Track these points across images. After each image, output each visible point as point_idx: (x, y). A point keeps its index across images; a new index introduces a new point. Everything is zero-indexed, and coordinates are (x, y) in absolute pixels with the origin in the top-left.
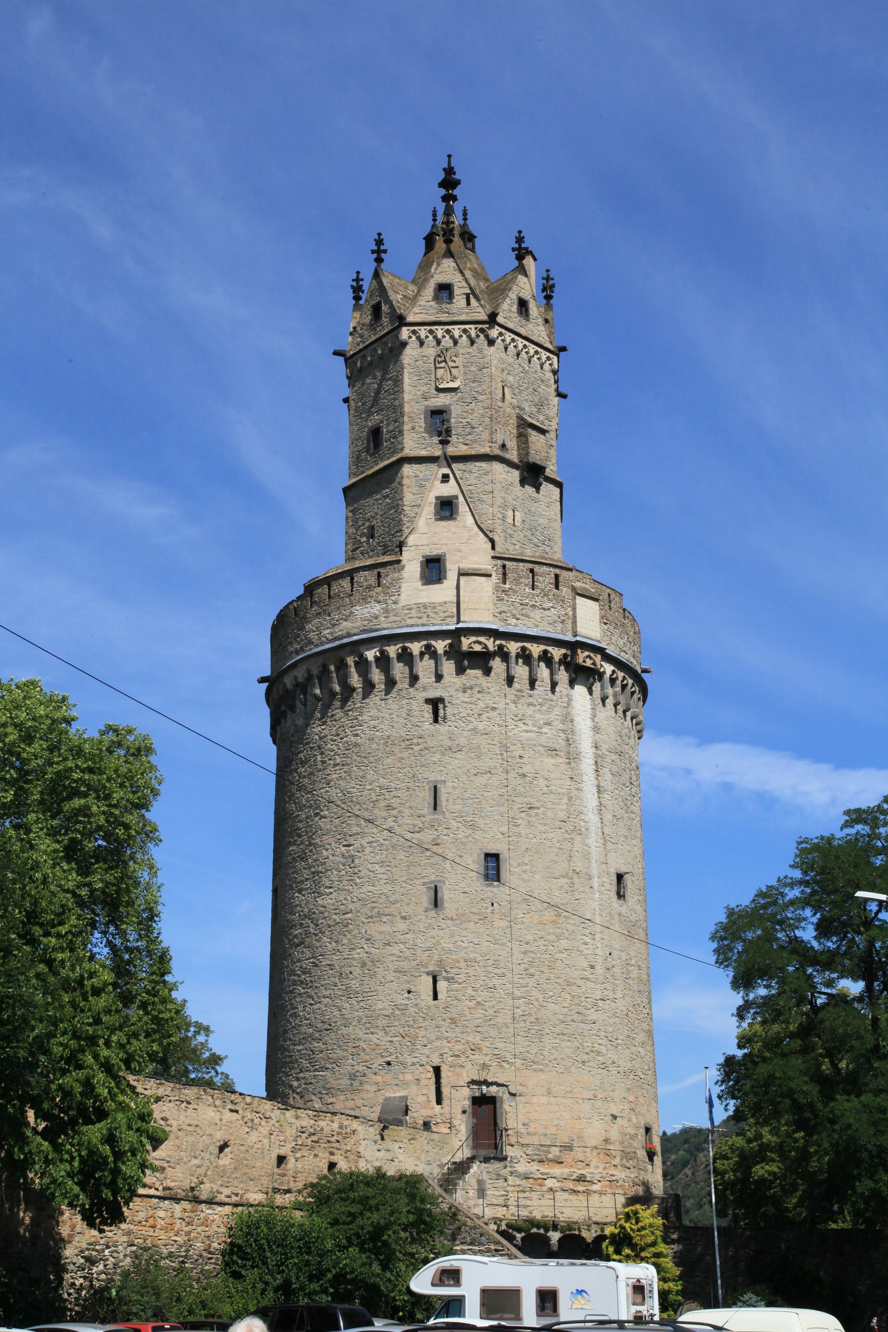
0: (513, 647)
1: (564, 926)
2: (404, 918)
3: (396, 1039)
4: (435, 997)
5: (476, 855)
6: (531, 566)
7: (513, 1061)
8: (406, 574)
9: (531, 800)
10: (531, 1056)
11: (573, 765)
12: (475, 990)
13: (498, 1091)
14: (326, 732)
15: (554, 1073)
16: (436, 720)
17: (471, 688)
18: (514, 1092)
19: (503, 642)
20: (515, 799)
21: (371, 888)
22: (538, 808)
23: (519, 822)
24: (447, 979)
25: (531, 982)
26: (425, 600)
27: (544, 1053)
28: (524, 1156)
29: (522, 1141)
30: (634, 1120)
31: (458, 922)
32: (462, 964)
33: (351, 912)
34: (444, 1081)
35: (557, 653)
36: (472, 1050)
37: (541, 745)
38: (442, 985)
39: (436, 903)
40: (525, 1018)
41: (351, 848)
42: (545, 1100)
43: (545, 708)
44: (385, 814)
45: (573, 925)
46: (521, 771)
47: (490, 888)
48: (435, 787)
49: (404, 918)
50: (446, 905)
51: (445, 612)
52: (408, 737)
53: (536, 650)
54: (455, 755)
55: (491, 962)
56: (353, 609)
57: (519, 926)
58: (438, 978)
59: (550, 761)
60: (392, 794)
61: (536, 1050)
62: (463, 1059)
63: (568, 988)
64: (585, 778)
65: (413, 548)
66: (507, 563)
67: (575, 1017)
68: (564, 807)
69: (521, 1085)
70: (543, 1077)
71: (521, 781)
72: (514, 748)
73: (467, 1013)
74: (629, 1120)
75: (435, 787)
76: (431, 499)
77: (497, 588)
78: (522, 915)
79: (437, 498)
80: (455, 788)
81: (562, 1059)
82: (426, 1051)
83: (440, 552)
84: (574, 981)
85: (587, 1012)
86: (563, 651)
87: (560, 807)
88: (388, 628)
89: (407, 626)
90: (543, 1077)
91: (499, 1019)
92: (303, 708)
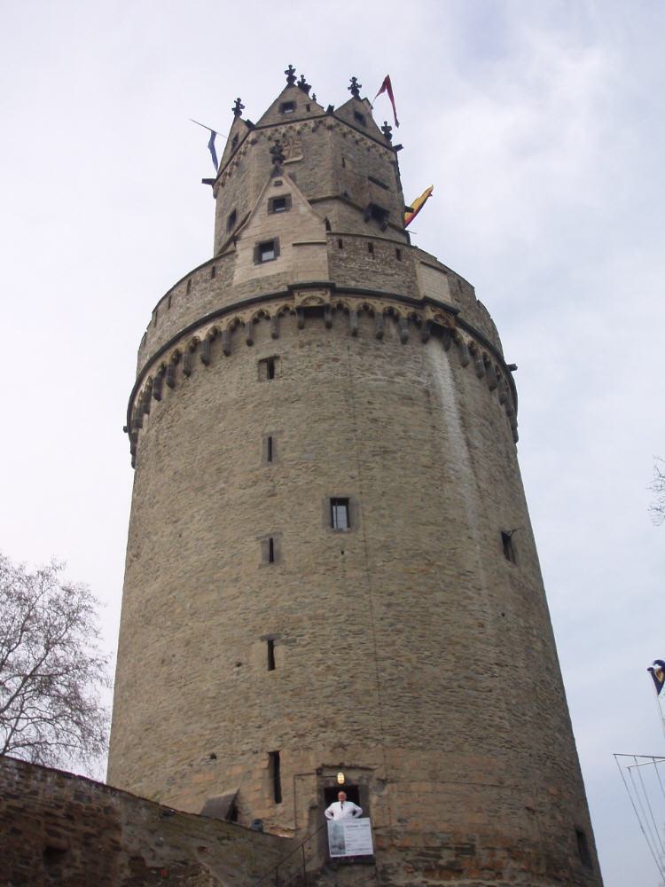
0: (354, 304)
1: (438, 576)
3: (222, 724)
4: (272, 666)
5: (319, 502)
6: (369, 241)
7: (380, 737)
8: (238, 261)
9: (386, 444)
10: (405, 731)
11: (434, 415)
12: (325, 652)
13: (361, 778)
15: (441, 751)
17: (309, 343)
18: (383, 778)
19: (343, 299)
20: (366, 443)
22: (395, 452)
23: (373, 465)
24: (286, 642)
25: (400, 640)
26: (259, 276)
27: (424, 726)
28: (404, 864)
29: (397, 842)
30: (560, 818)
31: (300, 576)
32: (307, 623)
33: (176, 589)
34: (283, 770)
35: (404, 311)
36: (322, 726)
37: (394, 393)
38: (280, 651)
40: (394, 683)
42: (428, 786)
43: (394, 361)
45: (451, 576)
46: (371, 416)
47: (337, 535)
48: (270, 439)
51: (279, 281)
53: (379, 306)
54: (293, 405)
55: (342, 618)
57: (378, 576)
58: (275, 643)
59: (406, 410)
60: (223, 456)
61: (412, 722)
62: (309, 739)
63: (450, 648)
64: (450, 429)
66: (341, 237)
67: (463, 682)
68: (427, 453)
69: (393, 768)
70: (424, 757)
71: (373, 425)
72: (362, 395)
73: (313, 680)
74: (553, 817)
75: (270, 439)
76: (266, 200)
77: (331, 258)
78: (381, 564)
79: (270, 199)
80: (292, 437)
81: (449, 733)
82: (261, 734)
83: (273, 237)
84: (458, 640)
85: (480, 677)
86: (411, 310)
87: (421, 452)
90: (424, 757)
91: (357, 686)
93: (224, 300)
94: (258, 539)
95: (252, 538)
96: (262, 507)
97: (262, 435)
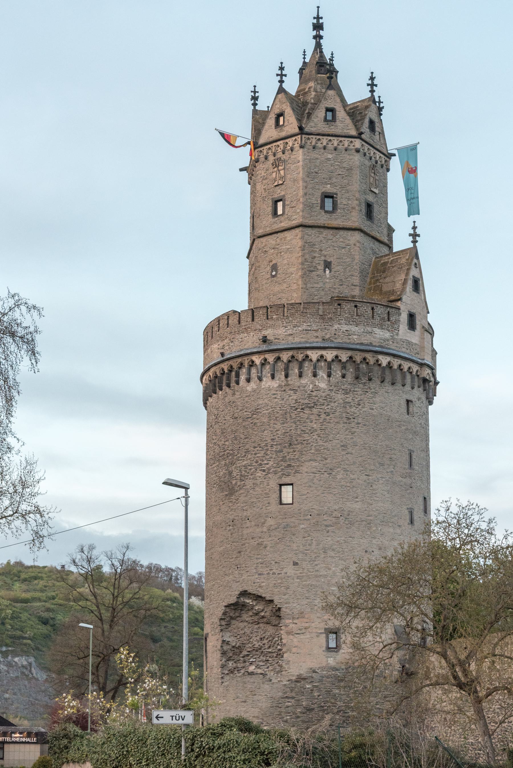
2: (399, 526)
14: (349, 400)
16: (408, 414)
21: (382, 505)
26: (409, 339)
39: (412, 522)
41: (370, 477)
44: (389, 463)
49: (399, 526)
50: (415, 523)
51: (416, 350)
52: (399, 420)
56: (375, 329)
60: (393, 451)
65: (404, 304)
88: (393, 350)
89: (402, 352)
92: (325, 377)
93: (395, 344)
94: (408, 509)
95: (405, 507)
96: (408, 492)
97: (408, 450)
